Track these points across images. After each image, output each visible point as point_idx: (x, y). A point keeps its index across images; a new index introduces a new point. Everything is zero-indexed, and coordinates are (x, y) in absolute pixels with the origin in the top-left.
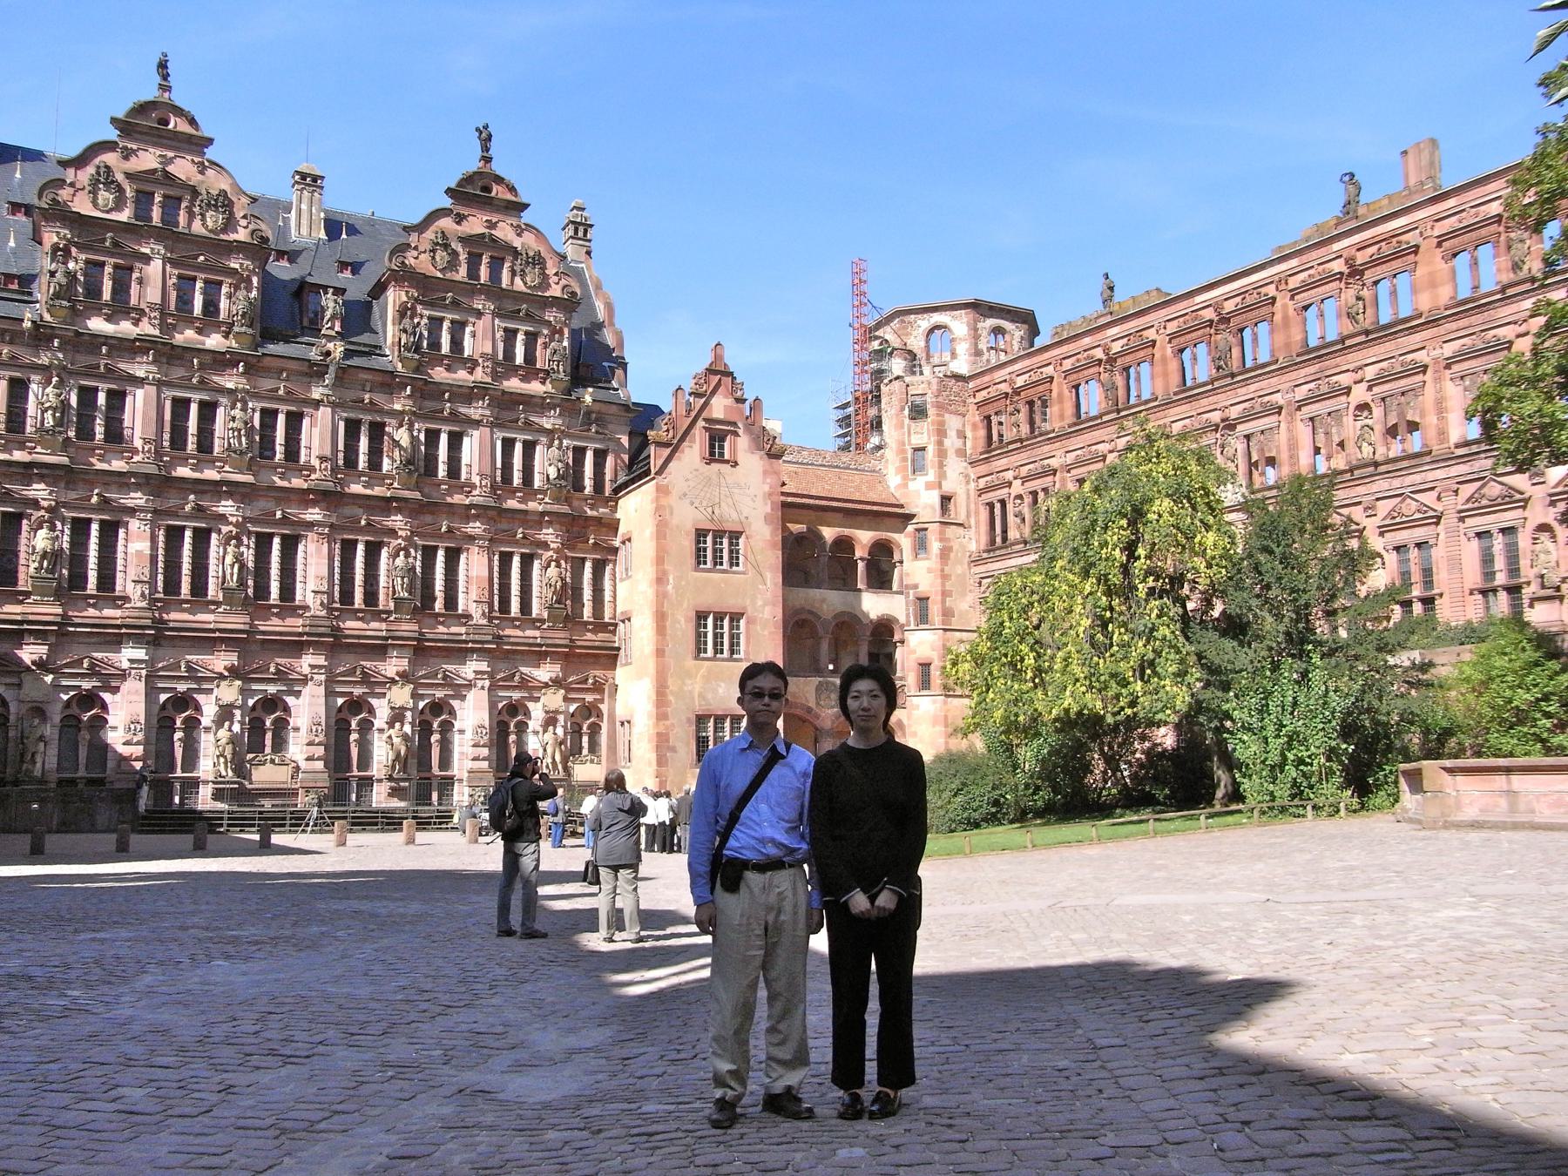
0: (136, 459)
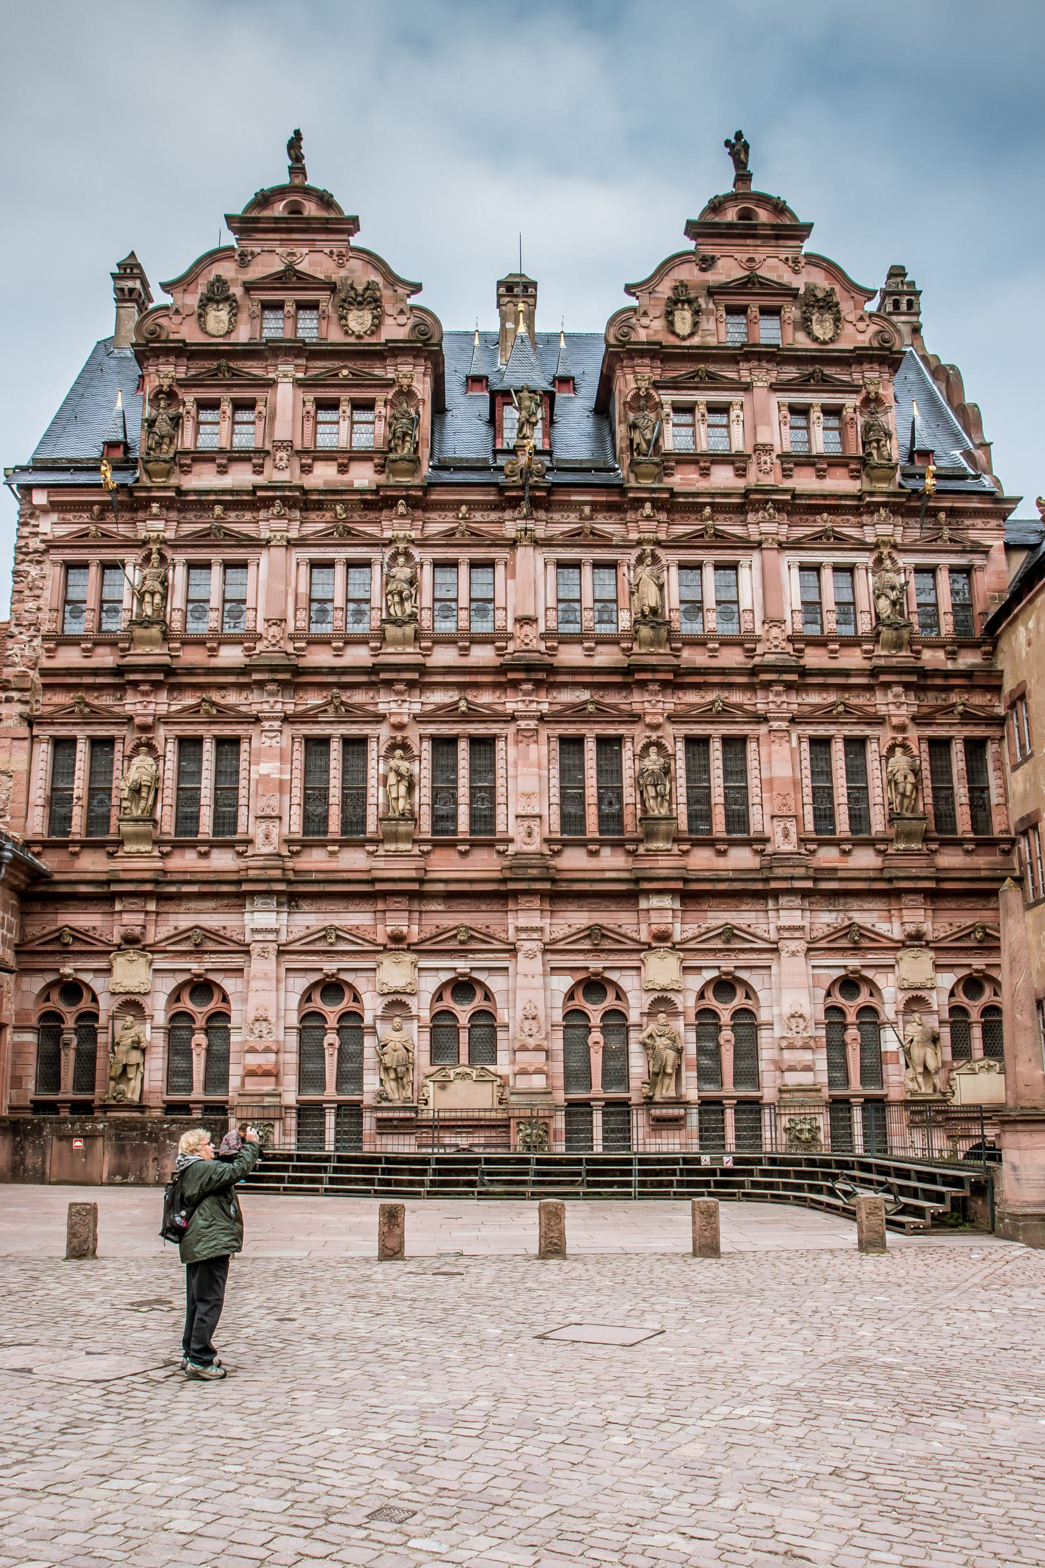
0: (260, 647)
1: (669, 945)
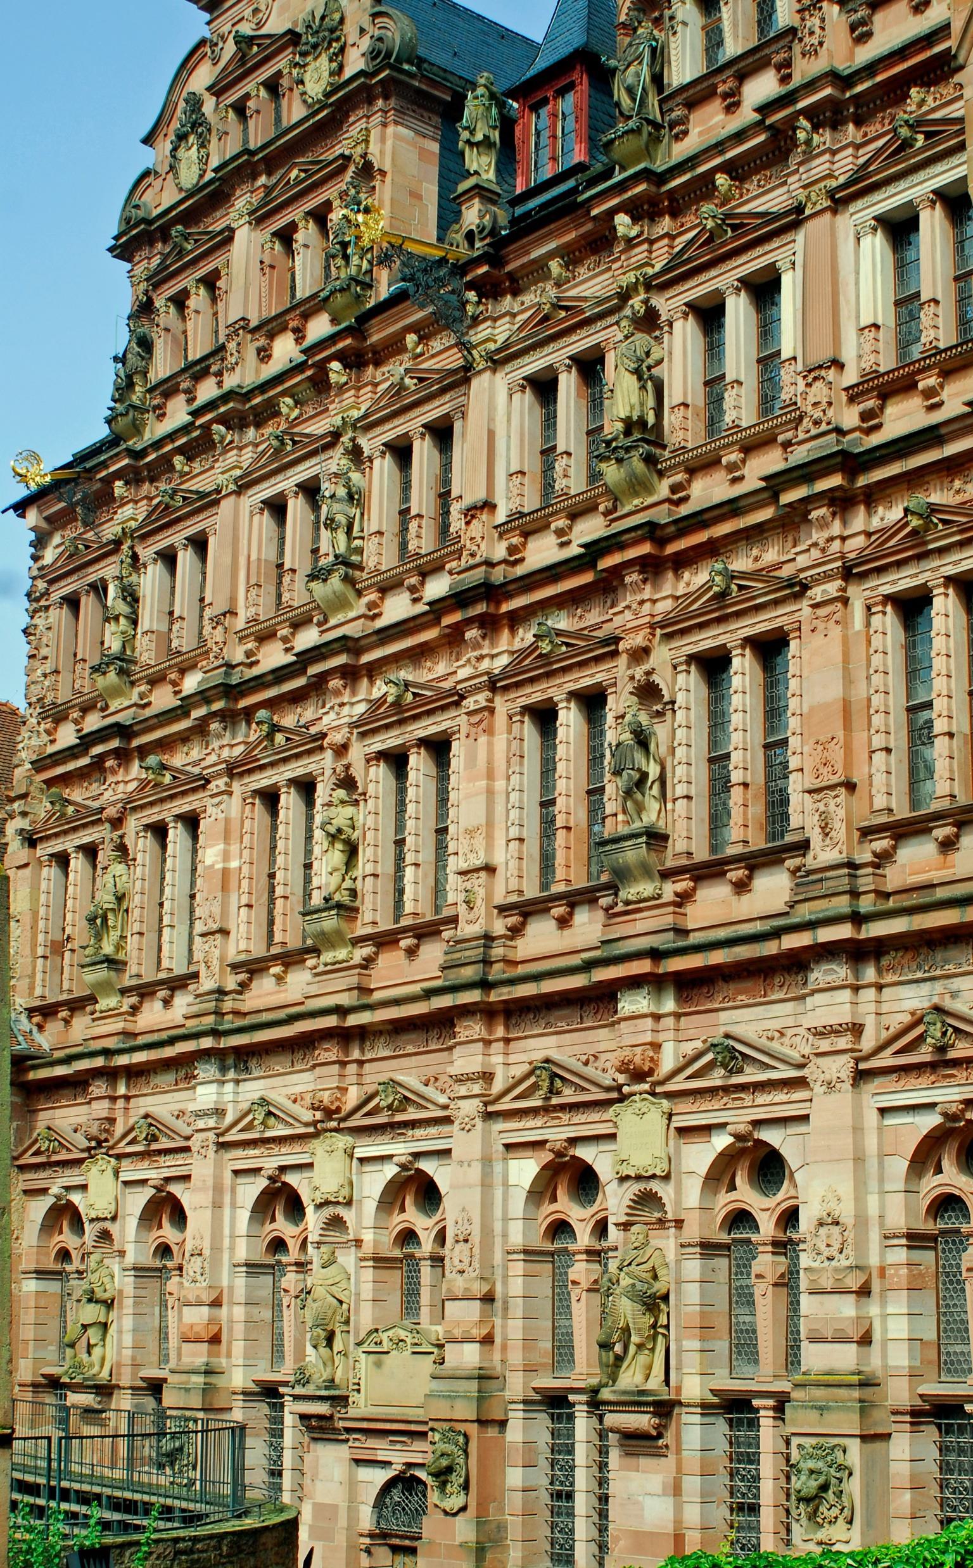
1: (646, 1087)
